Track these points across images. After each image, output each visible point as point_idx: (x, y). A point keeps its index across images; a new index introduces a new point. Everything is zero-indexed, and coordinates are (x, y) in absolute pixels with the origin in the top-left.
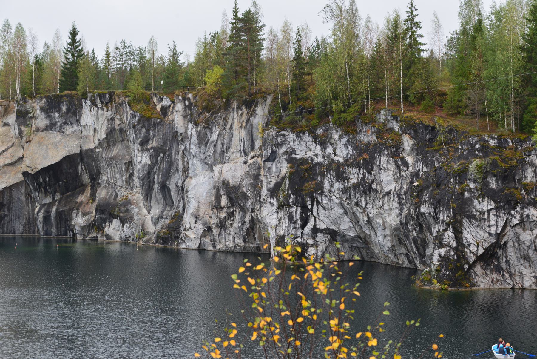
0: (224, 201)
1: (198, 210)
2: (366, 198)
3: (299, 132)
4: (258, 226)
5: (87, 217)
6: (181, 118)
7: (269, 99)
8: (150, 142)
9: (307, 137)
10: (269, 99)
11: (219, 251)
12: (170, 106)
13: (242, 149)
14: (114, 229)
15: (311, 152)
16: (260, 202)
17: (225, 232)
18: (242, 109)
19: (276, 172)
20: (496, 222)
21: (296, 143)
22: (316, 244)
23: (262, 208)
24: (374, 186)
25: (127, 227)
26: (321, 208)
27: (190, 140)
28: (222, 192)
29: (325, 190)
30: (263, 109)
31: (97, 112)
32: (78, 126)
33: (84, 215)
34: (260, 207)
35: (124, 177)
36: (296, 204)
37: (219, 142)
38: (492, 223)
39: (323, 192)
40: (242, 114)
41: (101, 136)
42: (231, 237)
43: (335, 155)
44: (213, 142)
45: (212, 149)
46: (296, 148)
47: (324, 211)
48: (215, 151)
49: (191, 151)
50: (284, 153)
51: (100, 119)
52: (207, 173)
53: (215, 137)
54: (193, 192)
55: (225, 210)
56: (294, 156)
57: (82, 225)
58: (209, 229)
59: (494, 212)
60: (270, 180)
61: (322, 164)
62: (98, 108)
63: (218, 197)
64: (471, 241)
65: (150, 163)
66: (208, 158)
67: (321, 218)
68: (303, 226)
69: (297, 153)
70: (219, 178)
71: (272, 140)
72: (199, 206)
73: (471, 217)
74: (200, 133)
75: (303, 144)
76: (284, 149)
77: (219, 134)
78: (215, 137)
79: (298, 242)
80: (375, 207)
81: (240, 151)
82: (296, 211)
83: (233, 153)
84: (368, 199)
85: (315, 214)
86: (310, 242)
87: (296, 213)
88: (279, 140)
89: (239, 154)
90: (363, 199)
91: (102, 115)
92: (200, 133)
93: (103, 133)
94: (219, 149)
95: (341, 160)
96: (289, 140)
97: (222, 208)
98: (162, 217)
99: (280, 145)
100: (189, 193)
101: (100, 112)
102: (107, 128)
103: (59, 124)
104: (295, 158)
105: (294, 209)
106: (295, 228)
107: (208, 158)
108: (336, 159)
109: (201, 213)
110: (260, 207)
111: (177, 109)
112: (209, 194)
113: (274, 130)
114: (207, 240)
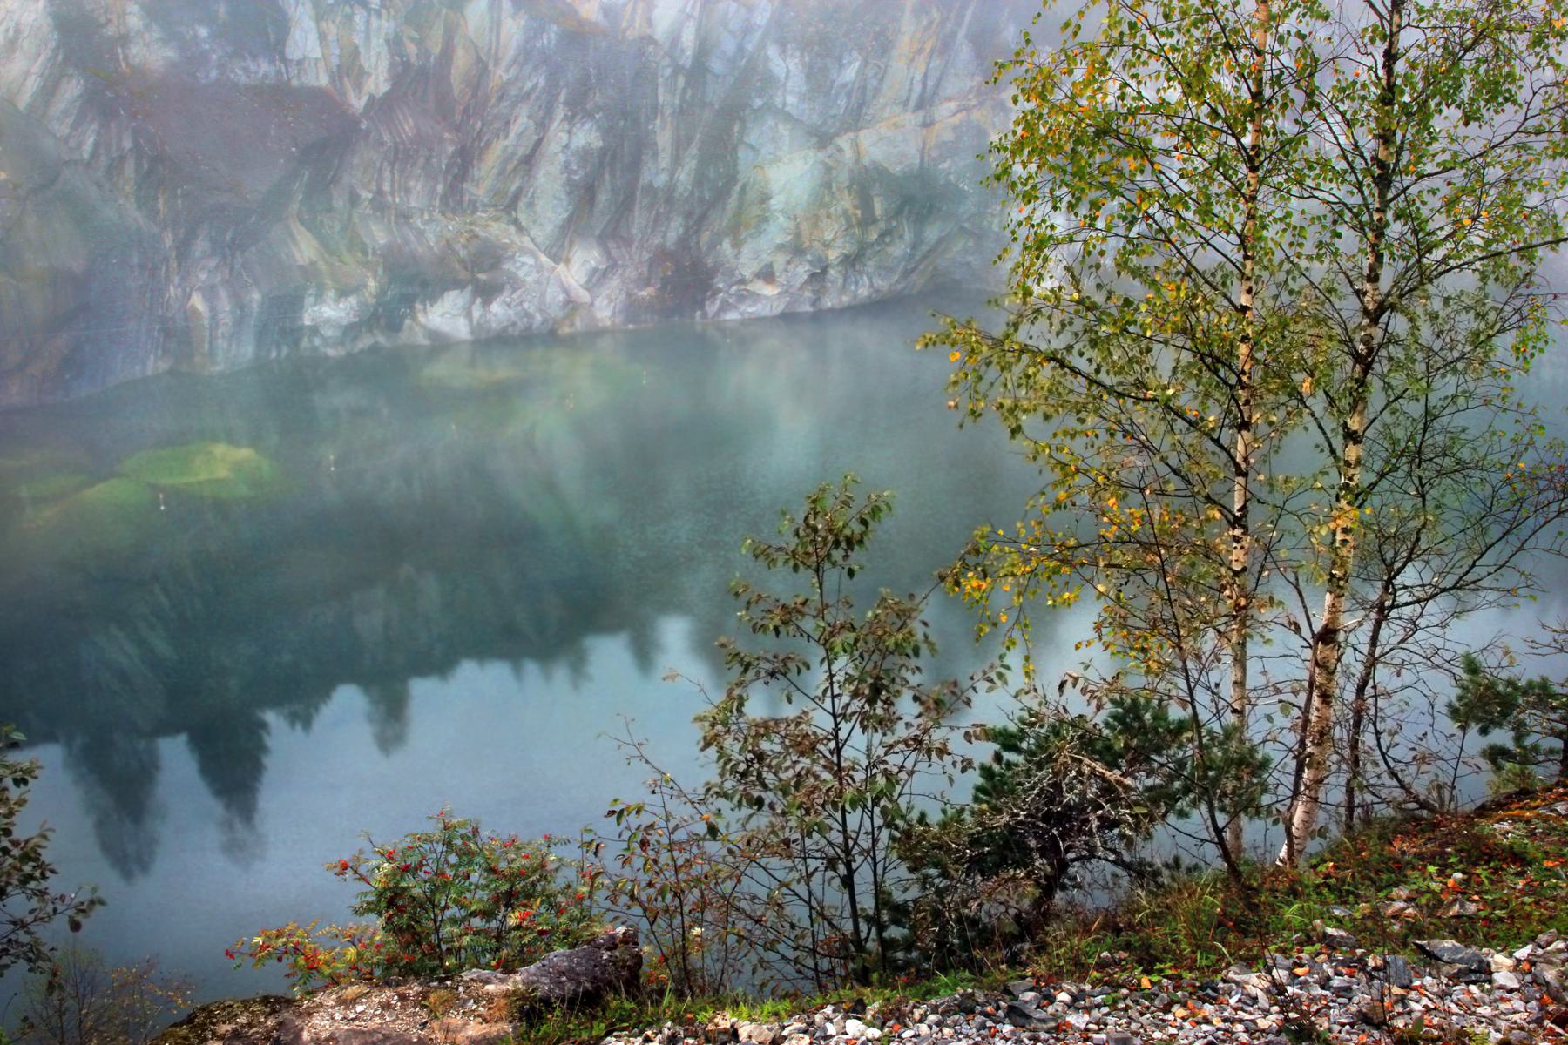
1: (798, 235)
5: (352, 301)
14: (447, 315)
27: (784, 85)
31: (368, 22)
32: (272, 62)
33: (343, 293)
35: (440, 188)
41: (377, 85)
44: (844, 86)
45: (842, 102)
51: (374, 41)
57: (345, 322)
58: (824, 270)
62: (369, 10)
63: (865, 202)
70: (857, 161)
81: (908, 100)
83: (884, 107)
91: (379, 29)
93: (382, 78)
97: (875, 221)
100: (772, 202)
101: (375, 22)
102: (392, 65)
103: (214, 57)
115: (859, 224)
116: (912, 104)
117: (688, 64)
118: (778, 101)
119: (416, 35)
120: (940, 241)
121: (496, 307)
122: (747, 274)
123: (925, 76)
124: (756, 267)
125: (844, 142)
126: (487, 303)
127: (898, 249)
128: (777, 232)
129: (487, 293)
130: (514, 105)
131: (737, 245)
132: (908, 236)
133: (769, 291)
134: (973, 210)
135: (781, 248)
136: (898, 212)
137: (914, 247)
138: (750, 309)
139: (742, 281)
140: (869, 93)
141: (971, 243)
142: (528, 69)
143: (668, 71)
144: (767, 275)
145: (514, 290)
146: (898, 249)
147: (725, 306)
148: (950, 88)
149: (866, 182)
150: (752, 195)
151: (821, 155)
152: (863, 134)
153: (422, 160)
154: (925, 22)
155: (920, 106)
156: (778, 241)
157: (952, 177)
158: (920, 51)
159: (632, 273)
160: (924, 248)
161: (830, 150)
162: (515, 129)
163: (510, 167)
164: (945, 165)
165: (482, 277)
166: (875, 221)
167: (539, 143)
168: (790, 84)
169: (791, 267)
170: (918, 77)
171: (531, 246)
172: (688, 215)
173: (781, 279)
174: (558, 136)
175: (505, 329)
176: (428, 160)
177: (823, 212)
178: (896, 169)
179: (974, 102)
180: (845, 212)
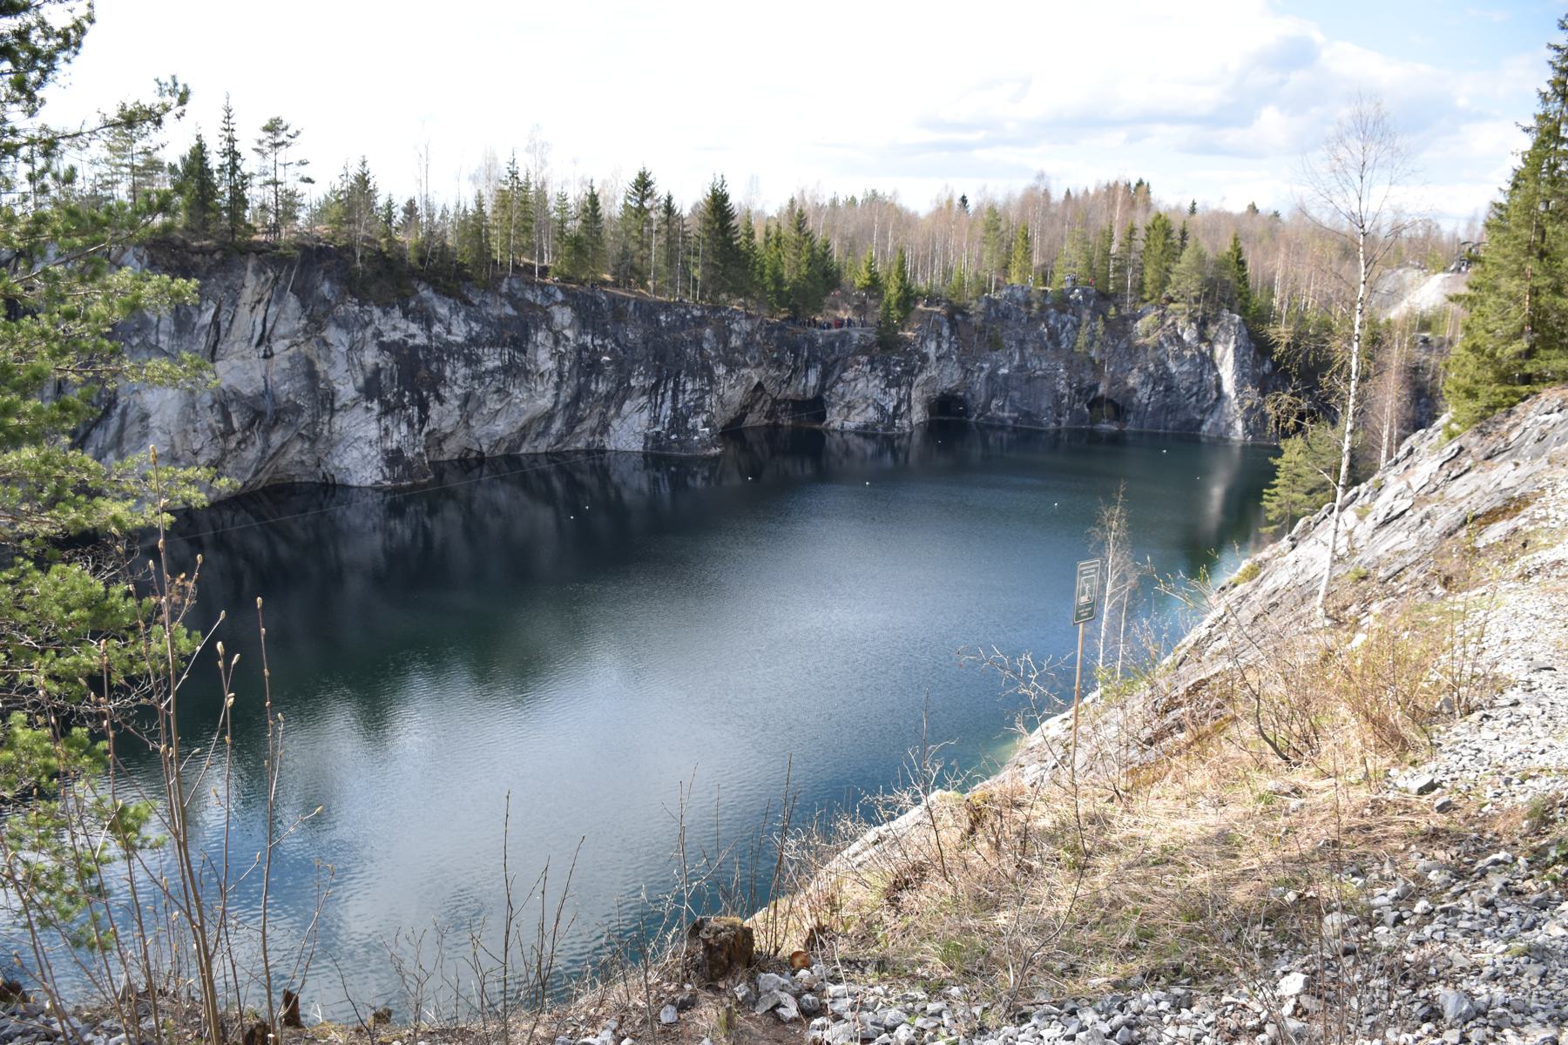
1: (173, 446)
3: (386, 308)
36: (412, 402)
43: (449, 332)
44: (204, 327)
45: (203, 339)
54: (158, 417)
63: (226, 417)
71: (356, 320)
77: (216, 315)
82: (414, 411)
95: (460, 339)
97: (234, 432)
99: (367, 324)
108: (451, 338)
115: (222, 435)
116: (255, 341)
118: (152, 339)
120: (283, 445)
123: (265, 320)
127: (251, 454)
131: (121, 456)
132: (259, 443)
134: (309, 420)
136: (252, 423)
137: (263, 452)
140: (222, 333)
141: (307, 446)
146: (251, 454)
148: (282, 329)
149: (224, 402)
150: (133, 414)
152: (218, 364)
155: (259, 344)
157: (292, 396)
158: (259, 301)
160: (271, 452)
166: (234, 432)
168: (162, 326)
170: (259, 320)
177: (190, 427)
178: (247, 391)
180: (210, 426)
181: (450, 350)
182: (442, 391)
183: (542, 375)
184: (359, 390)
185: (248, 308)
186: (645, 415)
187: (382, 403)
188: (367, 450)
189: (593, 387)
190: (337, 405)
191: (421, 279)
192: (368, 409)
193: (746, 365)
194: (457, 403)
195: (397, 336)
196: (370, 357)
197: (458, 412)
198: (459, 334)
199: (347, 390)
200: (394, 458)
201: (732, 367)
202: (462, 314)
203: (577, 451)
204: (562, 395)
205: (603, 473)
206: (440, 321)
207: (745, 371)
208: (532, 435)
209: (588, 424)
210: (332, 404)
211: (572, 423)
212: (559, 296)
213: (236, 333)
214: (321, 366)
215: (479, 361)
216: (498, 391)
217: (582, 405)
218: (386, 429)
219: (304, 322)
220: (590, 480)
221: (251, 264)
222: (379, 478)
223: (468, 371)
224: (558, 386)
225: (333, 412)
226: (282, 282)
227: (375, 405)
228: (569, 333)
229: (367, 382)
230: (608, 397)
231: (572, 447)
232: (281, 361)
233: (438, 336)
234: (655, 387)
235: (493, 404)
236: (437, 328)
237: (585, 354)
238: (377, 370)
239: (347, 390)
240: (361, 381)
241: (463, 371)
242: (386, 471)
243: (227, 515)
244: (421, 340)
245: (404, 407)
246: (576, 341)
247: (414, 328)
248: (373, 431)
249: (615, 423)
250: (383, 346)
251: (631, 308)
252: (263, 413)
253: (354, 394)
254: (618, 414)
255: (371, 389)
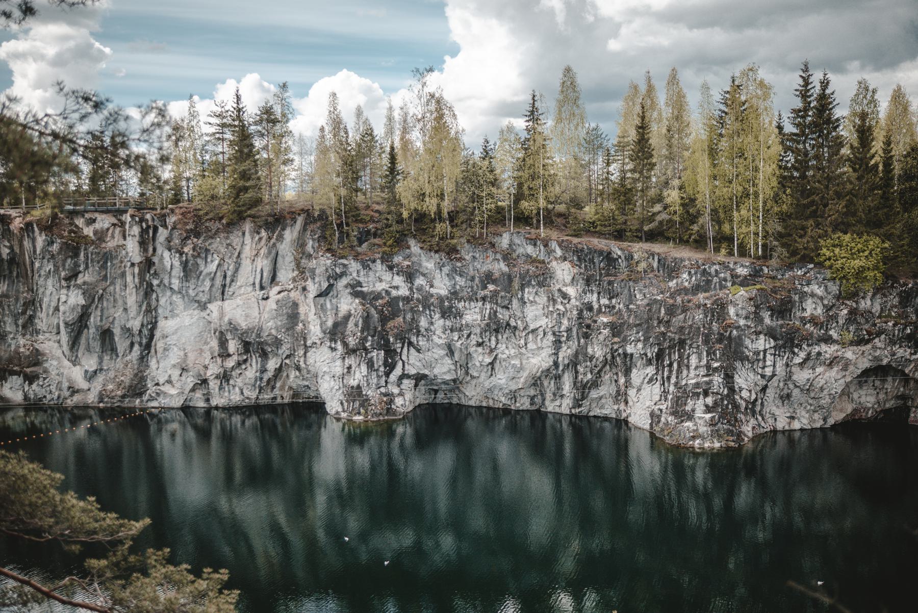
0: (233, 346)
2: (496, 337)
4: (285, 374)
6: (137, 244)
7: (300, 220)
8: (80, 276)
9: (379, 266)
10: (300, 220)
11: (217, 408)
12: (108, 229)
13: (257, 281)
15: (384, 284)
16: (306, 346)
17: (228, 384)
18: (258, 233)
19: (332, 309)
20: (774, 365)
21: (362, 273)
22: (401, 394)
23: (308, 354)
24: (513, 323)
25: (38, 385)
26: (412, 350)
28: (229, 336)
29: (422, 330)
30: (292, 232)
34: (305, 353)
35: (20, 322)
37: (218, 274)
38: (768, 363)
39: (419, 331)
40: (260, 239)
42: (237, 389)
43: (432, 286)
45: (208, 283)
46: (361, 279)
47: (417, 354)
48: (212, 286)
49: (172, 286)
50: (346, 287)
52: (196, 312)
53: (212, 267)
54: (175, 337)
55: (235, 358)
56: (359, 289)
58: (205, 382)
59: (772, 351)
60: (324, 319)
61: (408, 297)
63: (223, 343)
64: (743, 386)
65: (84, 302)
66: (201, 294)
67: (411, 362)
68: (387, 375)
69: (364, 285)
70: (221, 319)
72: (186, 355)
73: (744, 359)
74: (187, 261)
75: (371, 273)
76: (344, 281)
77: (219, 265)
78: (212, 267)
79: (381, 393)
80: (510, 347)
81: (254, 284)
82: (378, 356)
83: (241, 287)
84: (500, 337)
85: (404, 358)
86: (396, 391)
87: (378, 359)
88: (338, 270)
89: (250, 289)
90: (493, 338)
92: (187, 261)
94: (218, 281)
96: (351, 270)
97: (229, 355)
98: (101, 370)
104: (362, 292)
105: (374, 354)
106: (378, 376)
107: (201, 294)
108: (433, 291)
109: (190, 362)
110: (305, 353)
111: (132, 233)
112: (197, 339)
113: (328, 259)
114: (198, 394)
117: (137, 259)
118: (166, 282)
119: (8, 244)
120: (279, 371)
121: (34, 386)
122: (161, 381)
123: (262, 270)
124: (166, 378)
125: (214, 307)
126: (30, 384)
127: (251, 372)
128: (174, 357)
129: (31, 379)
130: (46, 280)
133: (173, 392)
134: (288, 352)
135: (174, 366)
136: (247, 351)
138: (163, 402)
139: (157, 384)
140: (228, 279)
141: (297, 373)
142: (45, 261)
143: (129, 264)
144: (169, 382)
145: (45, 379)
146: (251, 372)
147: (152, 399)
151: (204, 314)
152: (226, 303)
153: (6, 308)
154: (257, 238)
156: (173, 362)
157: (274, 332)
159: (112, 374)
160: (270, 374)
161: (208, 311)
162: (48, 292)
163: (51, 313)
164: (270, 324)
165: (28, 370)
166: (229, 355)
167: (59, 299)
168: (173, 273)
169: (183, 378)
170: (259, 270)
171: (61, 355)
172: (140, 344)
173: (178, 385)
174: (63, 298)
175: (40, 399)
176: (9, 306)
178: (244, 325)
179: (292, 286)
181: (426, 302)
182: (414, 339)
183: (533, 331)
184: (324, 332)
185: (248, 261)
186: (657, 389)
187: (345, 344)
188: (332, 383)
189: (590, 350)
190: (309, 343)
191: (415, 237)
192: (333, 349)
193: (828, 340)
194: (443, 352)
195: (380, 287)
196: (347, 304)
197: (448, 361)
198: (441, 287)
199: (315, 331)
200: (355, 394)
201: (788, 341)
202: (446, 270)
203: (606, 419)
204: (561, 355)
205: (622, 446)
206: (424, 275)
207: (829, 350)
208: (549, 396)
209: (603, 390)
210: (305, 339)
211: (583, 390)
212: (559, 252)
213: (241, 280)
214: (302, 310)
215: (460, 315)
216: (479, 345)
217: (581, 369)
218: (349, 368)
219: (296, 273)
220: (607, 452)
221: (248, 226)
222: (340, 409)
223: (448, 323)
224: (557, 344)
225: (306, 348)
226: (273, 241)
227: (339, 346)
228: (571, 291)
229: (336, 325)
230: (610, 362)
231: (597, 412)
232: (271, 304)
233: (420, 289)
234: (660, 356)
235: (480, 358)
236: (420, 281)
237: (586, 314)
238: (347, 317)
239: (315, 331)
240: (330, 323)
241: (439, 323)
242: (346, 404)
243: (237, 419)
244: (404, 291)
245: (365, 349)
246: (579, 298)
247: (399, 280)
248: (338, 368)
249: (632, 392)
250: (356, 295)
251: (655, 265)
252: (254, 346)
253: (321, 335)
254: (628, 384)
255: (335, 332)
